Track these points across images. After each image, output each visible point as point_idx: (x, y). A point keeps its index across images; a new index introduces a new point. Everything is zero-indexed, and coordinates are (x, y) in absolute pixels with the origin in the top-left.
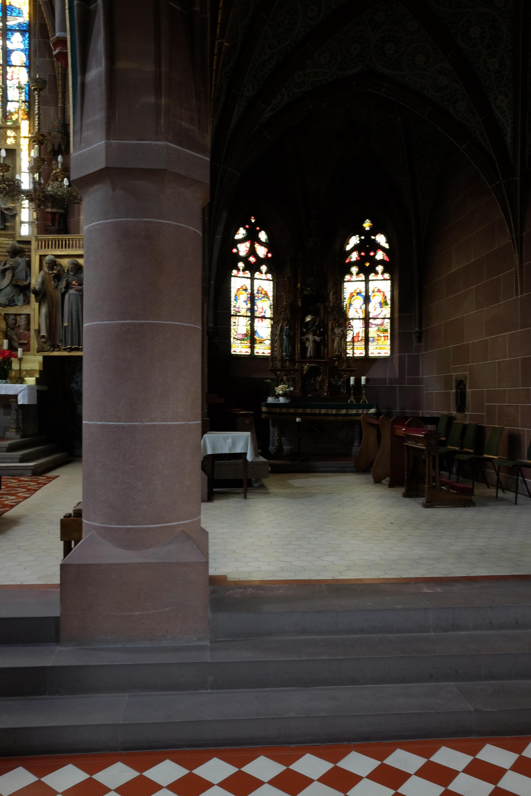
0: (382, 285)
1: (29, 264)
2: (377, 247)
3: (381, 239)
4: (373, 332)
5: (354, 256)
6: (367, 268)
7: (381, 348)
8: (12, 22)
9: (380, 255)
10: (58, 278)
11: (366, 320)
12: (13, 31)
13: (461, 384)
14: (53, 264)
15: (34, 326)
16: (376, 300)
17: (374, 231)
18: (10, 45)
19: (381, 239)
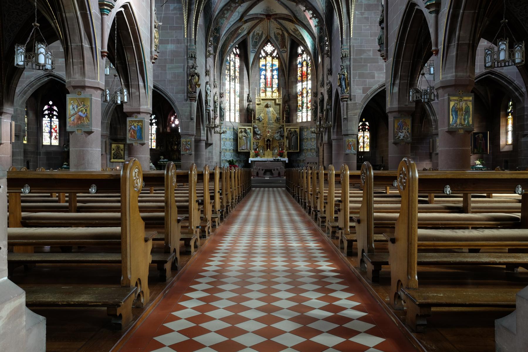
0: (367, 134)
1: (284, 130)
2: (366, 125)
3: (367, 123)
4: (365, 145)
5: (361, 127)
6: (364, 130)
7: (367, 149)
8: (274, 68)
9: (367, 127)
10: (291, 134)
11: (364, 143)
12: (274, 70)
13: (382, 158)
14: (290, 130)
15: (285, 145)
16: (366, 138)
17: (366, 121)
18: (273, 74)
19: (367, 123)
